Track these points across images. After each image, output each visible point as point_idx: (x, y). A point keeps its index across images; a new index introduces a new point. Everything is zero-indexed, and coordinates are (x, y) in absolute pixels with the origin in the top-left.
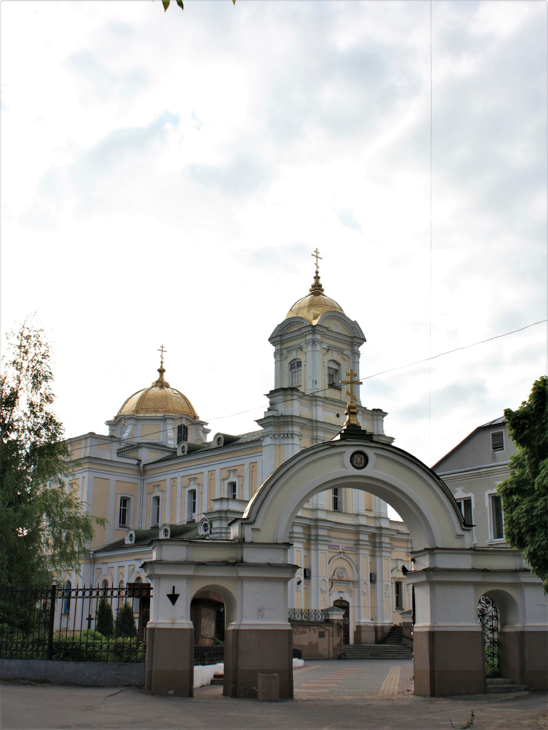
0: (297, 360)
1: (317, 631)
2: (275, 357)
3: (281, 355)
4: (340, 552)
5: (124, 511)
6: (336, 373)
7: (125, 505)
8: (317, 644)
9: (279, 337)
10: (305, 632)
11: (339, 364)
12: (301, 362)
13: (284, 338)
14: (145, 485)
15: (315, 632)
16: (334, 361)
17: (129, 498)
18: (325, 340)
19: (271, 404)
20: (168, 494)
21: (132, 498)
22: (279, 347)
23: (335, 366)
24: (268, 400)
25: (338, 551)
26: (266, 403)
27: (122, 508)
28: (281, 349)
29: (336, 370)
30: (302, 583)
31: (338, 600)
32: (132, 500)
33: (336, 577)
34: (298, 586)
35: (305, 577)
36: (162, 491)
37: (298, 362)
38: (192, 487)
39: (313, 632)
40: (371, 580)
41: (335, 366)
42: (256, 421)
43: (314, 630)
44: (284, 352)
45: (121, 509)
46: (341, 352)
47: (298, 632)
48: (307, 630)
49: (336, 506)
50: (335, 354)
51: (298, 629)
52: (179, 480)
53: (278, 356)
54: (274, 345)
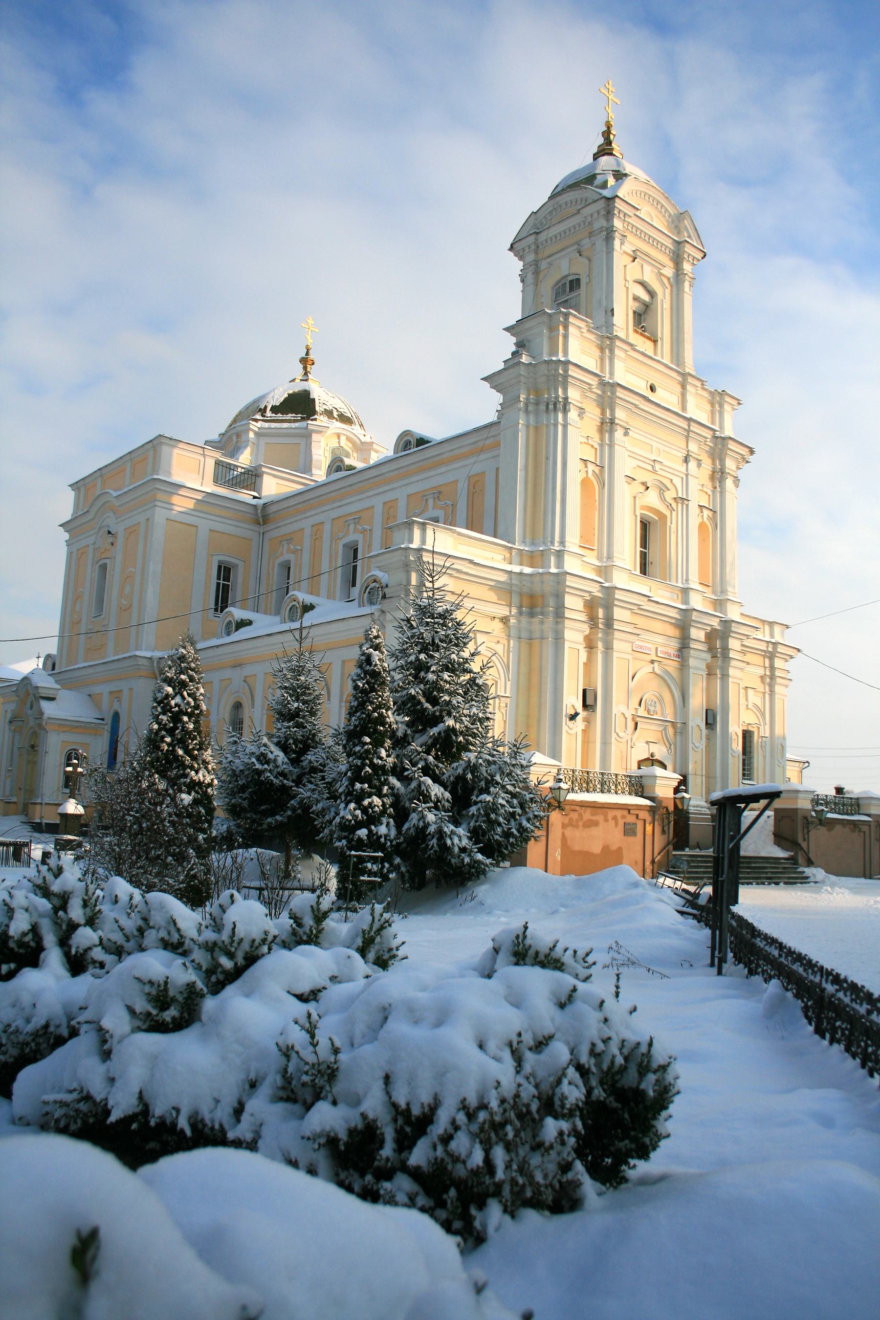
0: (570, 278)
1: (621, 823)
2: (522, 281)
3: (537, 273)
4: (652, 662)
5: (226, 588)
6: (645, 312)
7: (227, 578)
8: (620, 849)
9: (533, 237)
10: (596, 824)
11: (652, 294)
12: (578, 280)
13: (543, 237)
14: (266, 543)
15: (616, 825)
16: (643, 284)
17: (237, 566)
18: (630, 238)
19: (520, 345)
20: (306, 557)
21: (241, 565)
22: (531, 257)
23: (645, 297)
24: (514, 340)
25: (649, 658)
26: (509, 343)
27: (221, 582)
28: (536, 263)
29: (647, 306)
30: (579, 718)
31: (647, 759)
32: (241, 570)
33: (642, 712)
34: (571, 723)
35: (585, 706)
36: (295, 552)
37: (571, 282)
38: (351, 537)
39: (612, 823)
40: (707, 723)
41: (645, 297)
42: (484, 379)
43: (615, 818)
44: (544, 265)
45: (218, 584)
46: (657, 265)
47: (581, 824)
48: (600, 818)
49: (644, 571)
50: (647, 269)
51: (580, 815)
52: (327, 527)
53: (530, 278)
54: (521, 258)
